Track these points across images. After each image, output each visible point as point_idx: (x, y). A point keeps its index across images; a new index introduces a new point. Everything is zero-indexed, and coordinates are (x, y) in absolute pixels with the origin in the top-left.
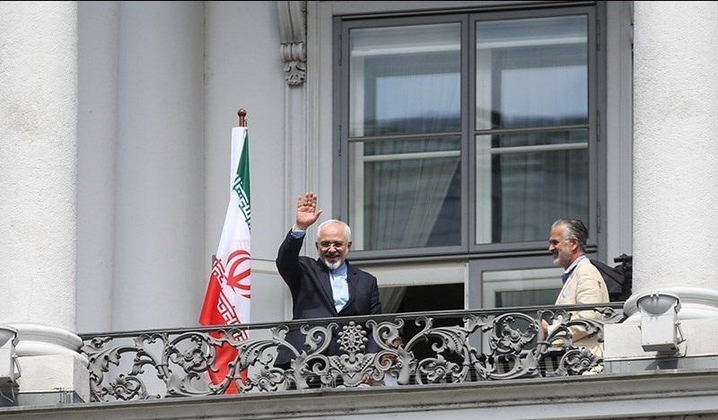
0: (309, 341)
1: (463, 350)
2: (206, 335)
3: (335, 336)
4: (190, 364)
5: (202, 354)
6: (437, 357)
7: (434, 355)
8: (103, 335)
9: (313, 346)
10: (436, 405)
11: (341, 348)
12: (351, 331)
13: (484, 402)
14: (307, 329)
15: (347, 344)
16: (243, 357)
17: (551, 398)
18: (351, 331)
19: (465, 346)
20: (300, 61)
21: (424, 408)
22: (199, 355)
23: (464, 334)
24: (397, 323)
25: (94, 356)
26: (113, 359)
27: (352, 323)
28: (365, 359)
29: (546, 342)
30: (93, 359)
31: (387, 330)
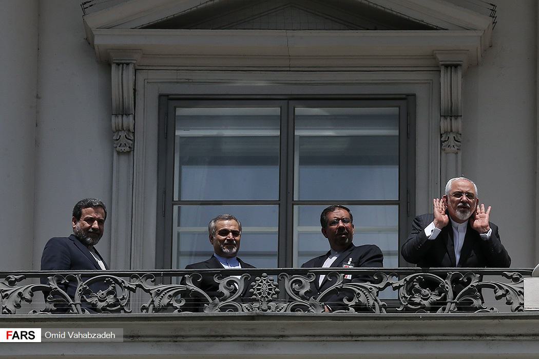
0: (222, 289)
1: (374, 305)
2: (120, 279)
3: (248, 286)
4: (104, 304)
5: (115, 296)
6: (348, 309)
7: (346, 307)
8: (17, 274)
9: (226, 293)
10: (365, 336)
11: (254, 297)
12: (264, 282)
13: (413, 335)
14: (220, 278)
15: (260, 294)
16: (157, 300)
17: (480, 335)
18: (264, 282)
19: (376, 300)
20: (129, 130)
21: (354, 339)
22: (112, 296)
23: (375, 290)
24: (309, 277)
25: (8, 293)
26: (27, 296)
27: (265, 274)
28: (277, 308)
29: (455, 300)
30: (7, 295)
31: (299, 282)
